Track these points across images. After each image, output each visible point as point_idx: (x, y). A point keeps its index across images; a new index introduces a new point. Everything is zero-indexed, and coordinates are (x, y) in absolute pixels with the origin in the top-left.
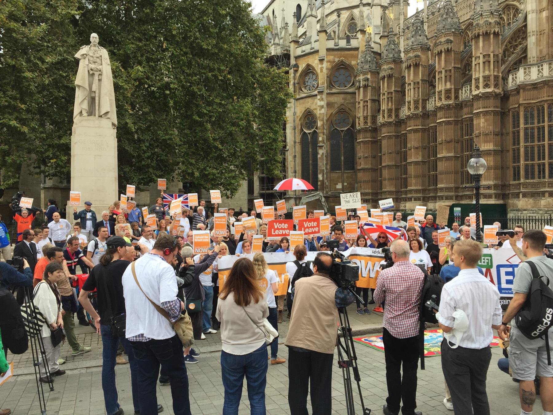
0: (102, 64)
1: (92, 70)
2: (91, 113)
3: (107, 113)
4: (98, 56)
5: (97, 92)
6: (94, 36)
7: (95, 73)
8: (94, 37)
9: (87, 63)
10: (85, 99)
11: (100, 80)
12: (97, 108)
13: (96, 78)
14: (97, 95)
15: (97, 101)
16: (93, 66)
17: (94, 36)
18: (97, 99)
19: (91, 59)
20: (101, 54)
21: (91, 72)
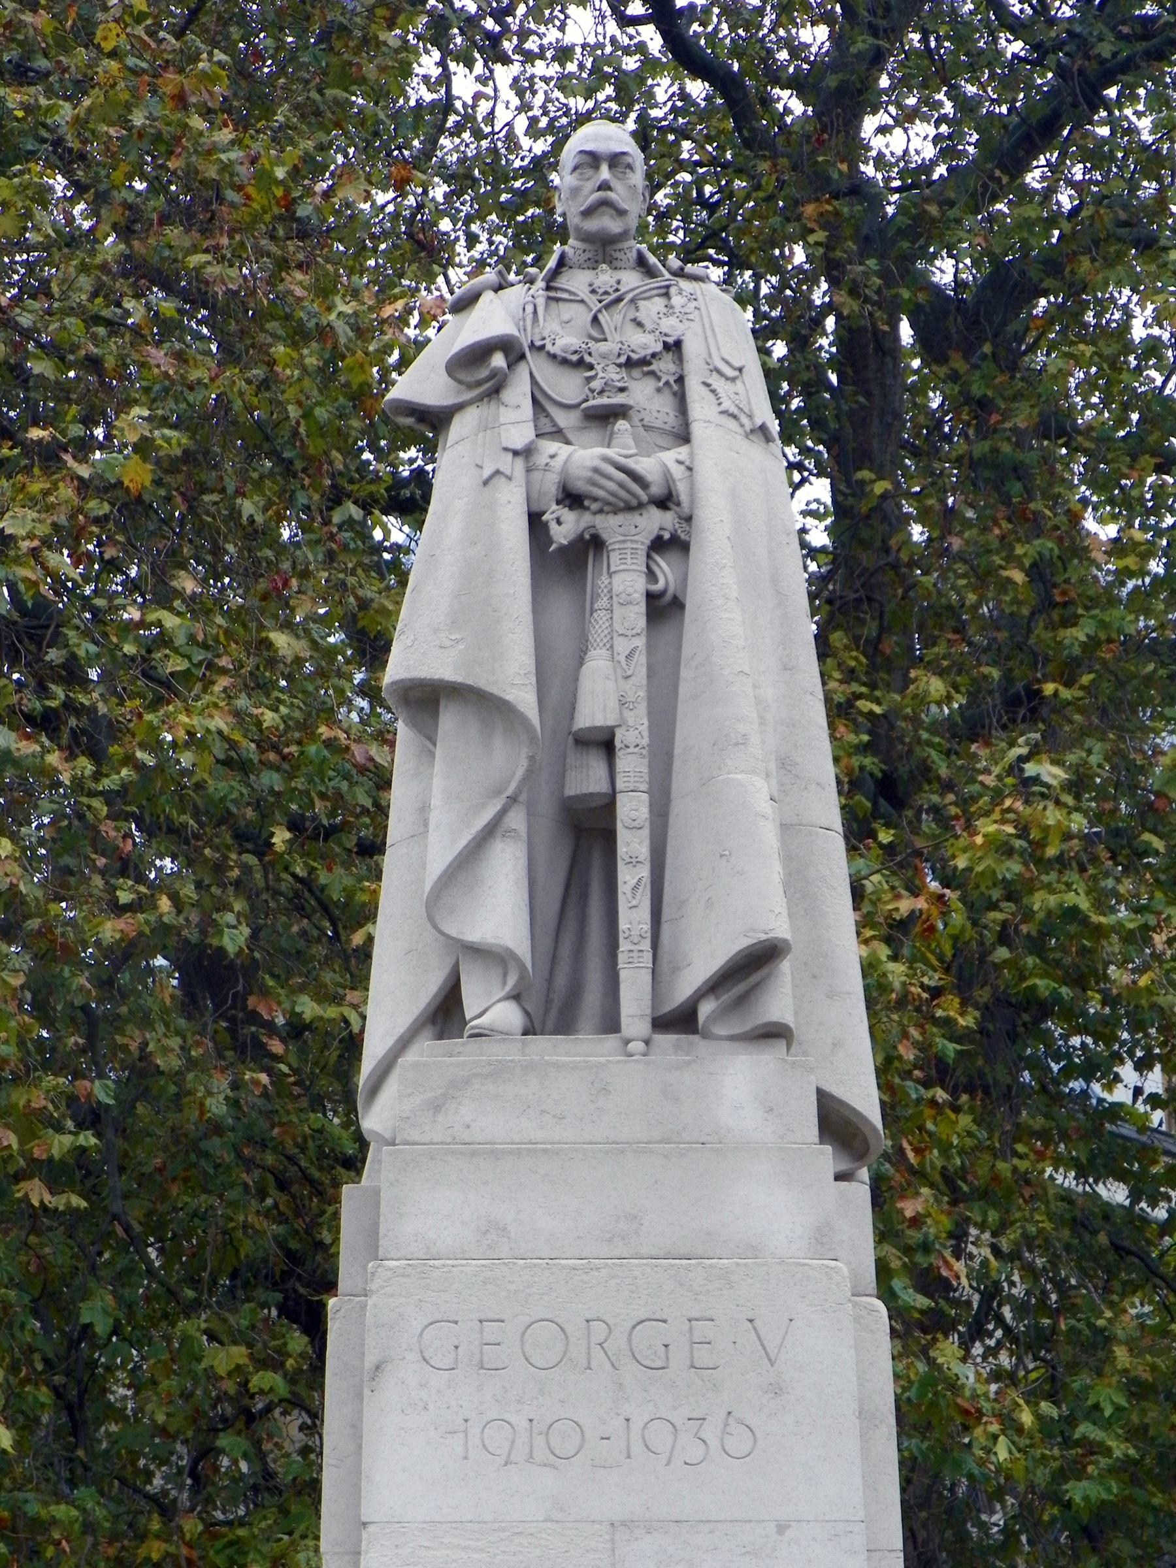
0: (684, 437)
1: (572, 498)
4: (644, 343)
5: (634, 735)
8: (592, 159)
9: (521, 434)
10: (490, 832)
12: (633, 917)
13: (624, 580)
14: (632, 767)
15: (632, 844)
18: (632, 810)
19: (566, 387)
20: (672, 327)
21: (565, 527)
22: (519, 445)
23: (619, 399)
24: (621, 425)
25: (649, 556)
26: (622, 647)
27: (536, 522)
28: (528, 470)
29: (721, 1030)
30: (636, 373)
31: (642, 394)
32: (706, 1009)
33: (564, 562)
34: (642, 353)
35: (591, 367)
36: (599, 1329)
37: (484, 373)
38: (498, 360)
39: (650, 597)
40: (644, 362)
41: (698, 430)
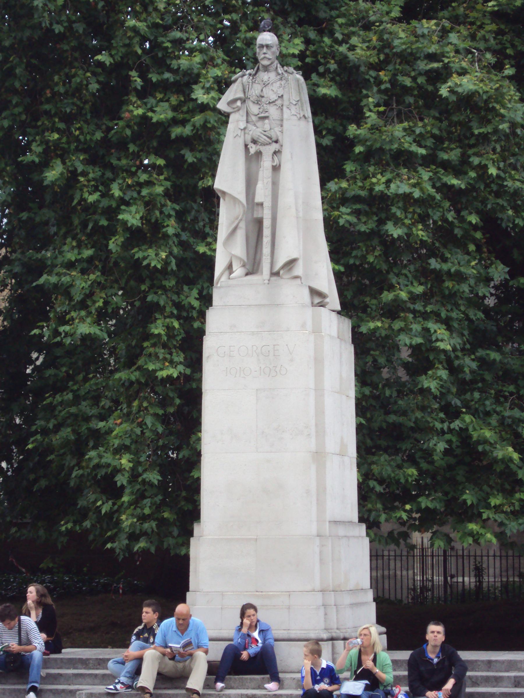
1: (254, 142)
2: (253, 268)
3: (291, 263)
11: (276, 169)
12: (266, 250)
13: (267, 163)
15: (267, 232)
18: (267, 223)
19: (254, 109)
21: (253, 149)
24: (267, 121)
26: (265, 181)
28: (245, 134)
29: (285, 277)
30: (271, 105)
31: (273, 111)
32: (281, 272)
33: (253, 159)
36: (255, 348)
38: (239, 103)
40: (273, 102)
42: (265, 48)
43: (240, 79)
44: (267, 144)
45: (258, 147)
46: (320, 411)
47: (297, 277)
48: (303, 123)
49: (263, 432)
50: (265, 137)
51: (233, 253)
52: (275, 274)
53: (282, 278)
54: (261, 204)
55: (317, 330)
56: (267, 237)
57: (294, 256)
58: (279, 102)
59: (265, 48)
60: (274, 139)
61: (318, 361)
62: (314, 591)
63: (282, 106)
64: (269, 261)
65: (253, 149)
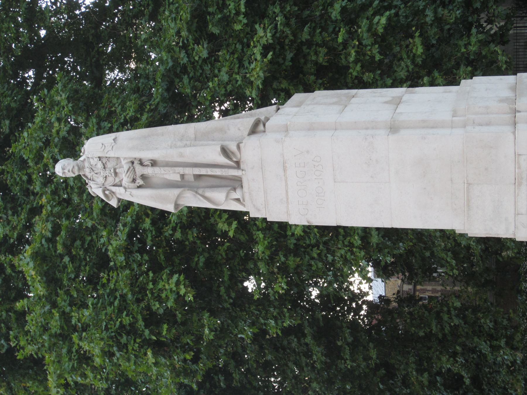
0: (118, 158)
1: (134, 181)
2: (236, 183)
3: (225, 152)
4: (100, 165)
6: (64, 168)
7: (139, 173)
12: (218, 172)
13: (149, 171)
15: (203, 171)
16: (126, 181)
17: (64, 168)
21: (140, 182)
22: (124, 190)
23: (112, 171)
24: (117, 171)
25: (144, 166)
26: (163, 172)
27: (139, 187)
29: (239, 156)
30: (106, 166)
32: (235, 160)
33: (146, 182)
34: (102, 165)
35: (106, 176)
37: (110, 195)
38: (107, 192)
39: (152, 165)
41: (116, 156)
42: (65, 171)
43: (93, 190)
44: (135, 170)
45: (138, 177)
46: (354, 126)
47: (238, 147)
48: (119, 141)
49: (372, 177)
50: (128, 173)
51: (224, 199)
52: (238, 163)
53: (240, 159)
54: (182, 176)
55: (286, 129)
56: (207, 172)
57: (219, 149)
58: (104, 161)
59: (65, 171)
60: (130, 165)
61: (311, 128)
62: (514, 133)
63: (107, 157)
64: (226, 170)
65: (140, 182)
